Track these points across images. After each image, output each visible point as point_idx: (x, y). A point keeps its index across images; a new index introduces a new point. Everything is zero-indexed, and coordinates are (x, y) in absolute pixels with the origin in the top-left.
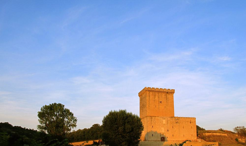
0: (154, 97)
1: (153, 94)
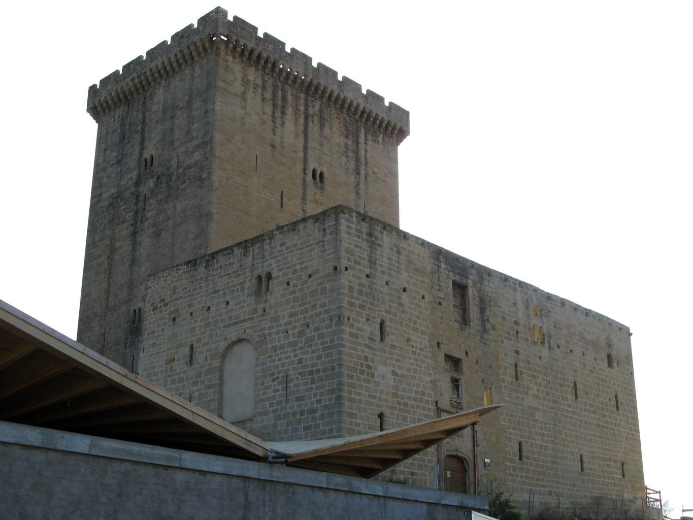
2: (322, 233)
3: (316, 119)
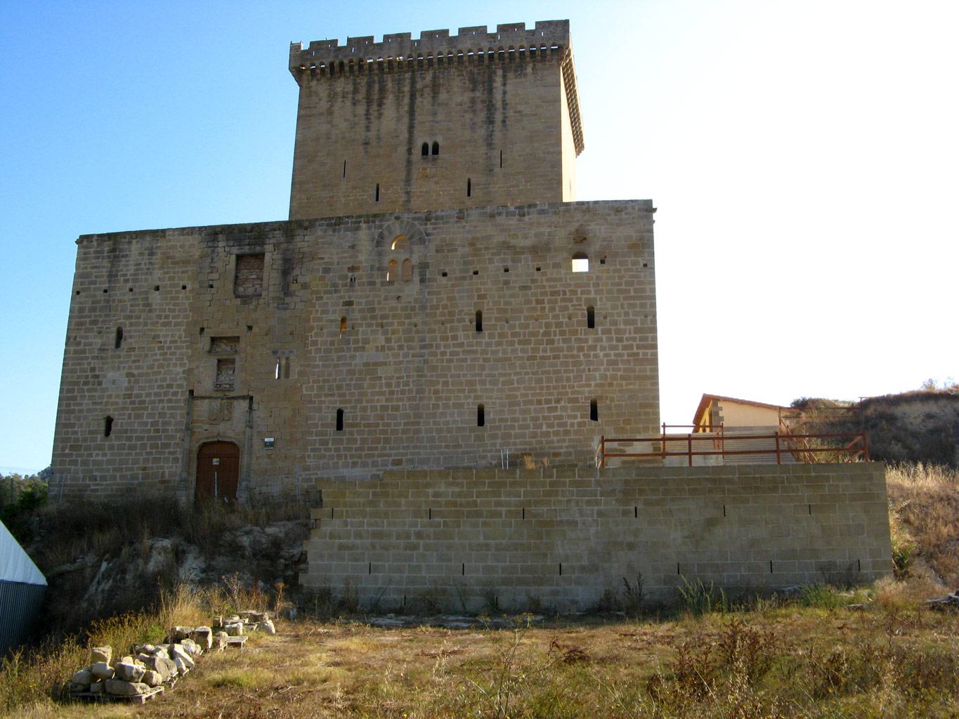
0: (368, 114)
1: (363, 90)
3: (427, 91)
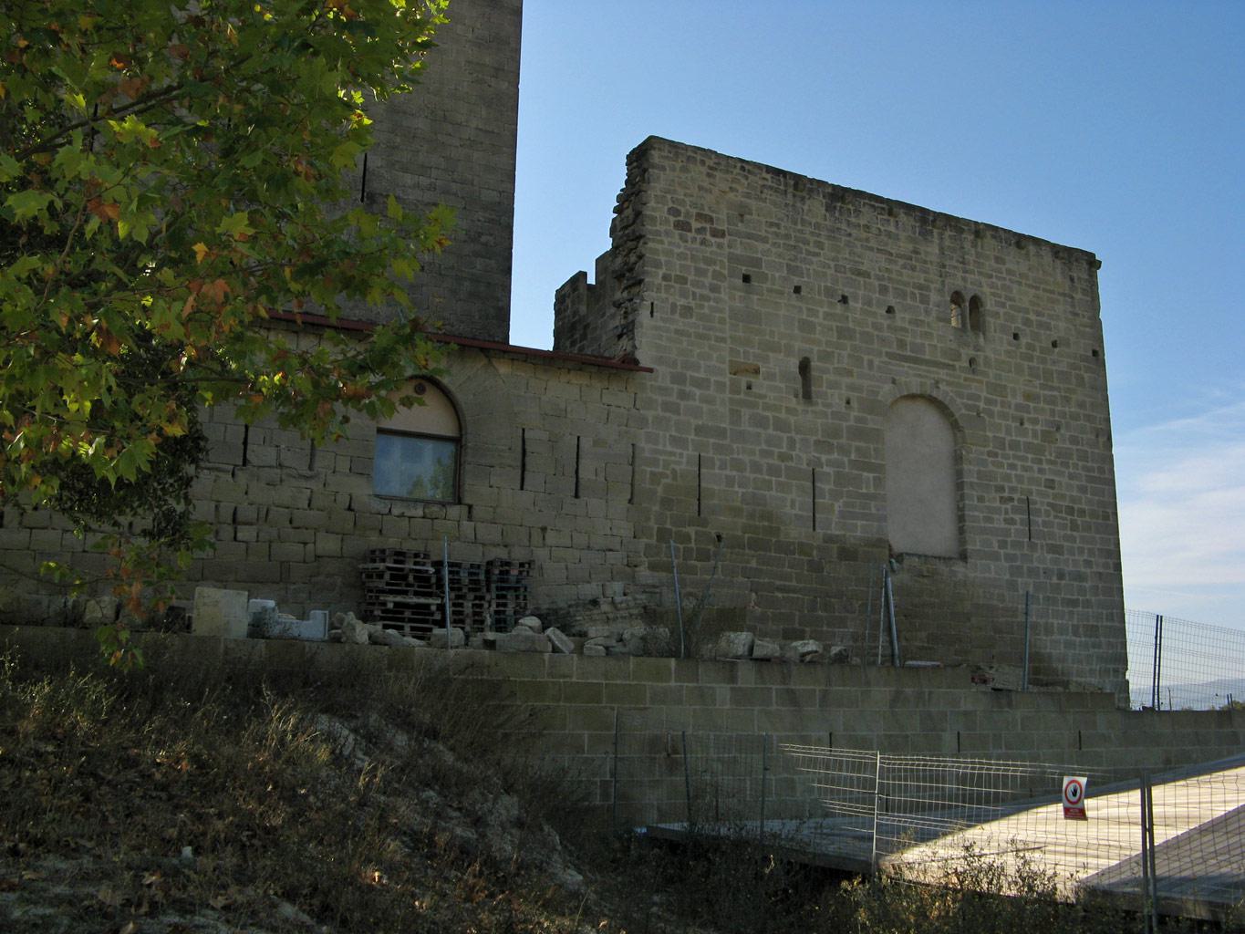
2: (1068, 283)
